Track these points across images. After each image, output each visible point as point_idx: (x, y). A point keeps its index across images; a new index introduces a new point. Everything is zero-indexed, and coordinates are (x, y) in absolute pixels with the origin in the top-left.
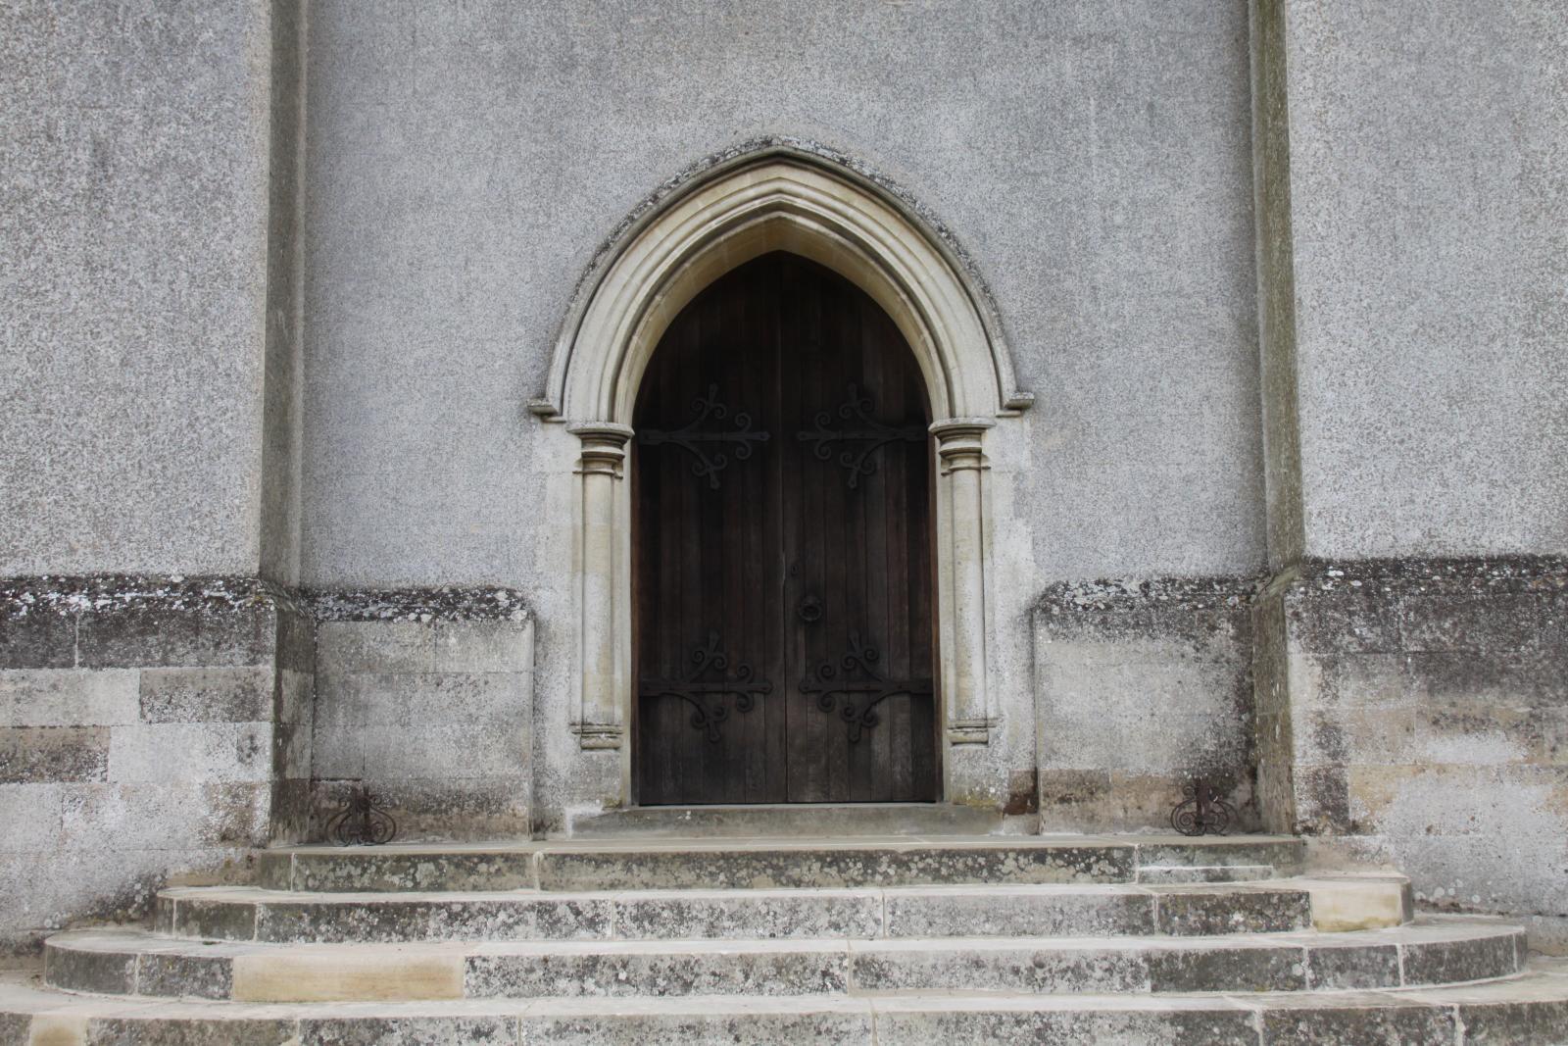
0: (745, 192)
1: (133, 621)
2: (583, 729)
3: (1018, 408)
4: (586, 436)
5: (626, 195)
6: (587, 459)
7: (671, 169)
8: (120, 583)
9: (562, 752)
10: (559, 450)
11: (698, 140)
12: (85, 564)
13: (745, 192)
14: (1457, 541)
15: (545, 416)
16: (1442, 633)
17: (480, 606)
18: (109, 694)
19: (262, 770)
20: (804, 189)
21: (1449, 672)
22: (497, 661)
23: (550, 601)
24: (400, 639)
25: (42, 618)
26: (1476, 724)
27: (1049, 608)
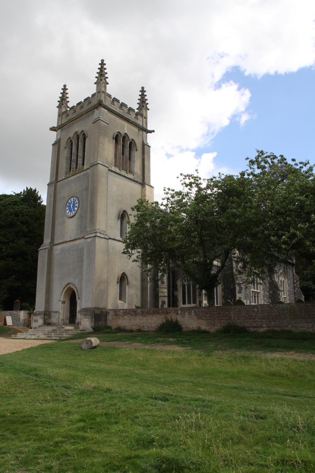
0: (68, 286)
2: (61, 320)
3: (79, 299)
4: (62, 302)
5: (64, 286)
8: (40, 311)
9: (60, 321)
10: (61, 303)
11: (66, 283)
12: (39, 311)
15: (60, 301)
16: (85, 313)
17: (56, 312)
18: (38, 317)
19: (43, 322)
20: (71, 285)
21: (85, 315)
22: (57, 315)
23: (60, 312)
26: (86, 318)
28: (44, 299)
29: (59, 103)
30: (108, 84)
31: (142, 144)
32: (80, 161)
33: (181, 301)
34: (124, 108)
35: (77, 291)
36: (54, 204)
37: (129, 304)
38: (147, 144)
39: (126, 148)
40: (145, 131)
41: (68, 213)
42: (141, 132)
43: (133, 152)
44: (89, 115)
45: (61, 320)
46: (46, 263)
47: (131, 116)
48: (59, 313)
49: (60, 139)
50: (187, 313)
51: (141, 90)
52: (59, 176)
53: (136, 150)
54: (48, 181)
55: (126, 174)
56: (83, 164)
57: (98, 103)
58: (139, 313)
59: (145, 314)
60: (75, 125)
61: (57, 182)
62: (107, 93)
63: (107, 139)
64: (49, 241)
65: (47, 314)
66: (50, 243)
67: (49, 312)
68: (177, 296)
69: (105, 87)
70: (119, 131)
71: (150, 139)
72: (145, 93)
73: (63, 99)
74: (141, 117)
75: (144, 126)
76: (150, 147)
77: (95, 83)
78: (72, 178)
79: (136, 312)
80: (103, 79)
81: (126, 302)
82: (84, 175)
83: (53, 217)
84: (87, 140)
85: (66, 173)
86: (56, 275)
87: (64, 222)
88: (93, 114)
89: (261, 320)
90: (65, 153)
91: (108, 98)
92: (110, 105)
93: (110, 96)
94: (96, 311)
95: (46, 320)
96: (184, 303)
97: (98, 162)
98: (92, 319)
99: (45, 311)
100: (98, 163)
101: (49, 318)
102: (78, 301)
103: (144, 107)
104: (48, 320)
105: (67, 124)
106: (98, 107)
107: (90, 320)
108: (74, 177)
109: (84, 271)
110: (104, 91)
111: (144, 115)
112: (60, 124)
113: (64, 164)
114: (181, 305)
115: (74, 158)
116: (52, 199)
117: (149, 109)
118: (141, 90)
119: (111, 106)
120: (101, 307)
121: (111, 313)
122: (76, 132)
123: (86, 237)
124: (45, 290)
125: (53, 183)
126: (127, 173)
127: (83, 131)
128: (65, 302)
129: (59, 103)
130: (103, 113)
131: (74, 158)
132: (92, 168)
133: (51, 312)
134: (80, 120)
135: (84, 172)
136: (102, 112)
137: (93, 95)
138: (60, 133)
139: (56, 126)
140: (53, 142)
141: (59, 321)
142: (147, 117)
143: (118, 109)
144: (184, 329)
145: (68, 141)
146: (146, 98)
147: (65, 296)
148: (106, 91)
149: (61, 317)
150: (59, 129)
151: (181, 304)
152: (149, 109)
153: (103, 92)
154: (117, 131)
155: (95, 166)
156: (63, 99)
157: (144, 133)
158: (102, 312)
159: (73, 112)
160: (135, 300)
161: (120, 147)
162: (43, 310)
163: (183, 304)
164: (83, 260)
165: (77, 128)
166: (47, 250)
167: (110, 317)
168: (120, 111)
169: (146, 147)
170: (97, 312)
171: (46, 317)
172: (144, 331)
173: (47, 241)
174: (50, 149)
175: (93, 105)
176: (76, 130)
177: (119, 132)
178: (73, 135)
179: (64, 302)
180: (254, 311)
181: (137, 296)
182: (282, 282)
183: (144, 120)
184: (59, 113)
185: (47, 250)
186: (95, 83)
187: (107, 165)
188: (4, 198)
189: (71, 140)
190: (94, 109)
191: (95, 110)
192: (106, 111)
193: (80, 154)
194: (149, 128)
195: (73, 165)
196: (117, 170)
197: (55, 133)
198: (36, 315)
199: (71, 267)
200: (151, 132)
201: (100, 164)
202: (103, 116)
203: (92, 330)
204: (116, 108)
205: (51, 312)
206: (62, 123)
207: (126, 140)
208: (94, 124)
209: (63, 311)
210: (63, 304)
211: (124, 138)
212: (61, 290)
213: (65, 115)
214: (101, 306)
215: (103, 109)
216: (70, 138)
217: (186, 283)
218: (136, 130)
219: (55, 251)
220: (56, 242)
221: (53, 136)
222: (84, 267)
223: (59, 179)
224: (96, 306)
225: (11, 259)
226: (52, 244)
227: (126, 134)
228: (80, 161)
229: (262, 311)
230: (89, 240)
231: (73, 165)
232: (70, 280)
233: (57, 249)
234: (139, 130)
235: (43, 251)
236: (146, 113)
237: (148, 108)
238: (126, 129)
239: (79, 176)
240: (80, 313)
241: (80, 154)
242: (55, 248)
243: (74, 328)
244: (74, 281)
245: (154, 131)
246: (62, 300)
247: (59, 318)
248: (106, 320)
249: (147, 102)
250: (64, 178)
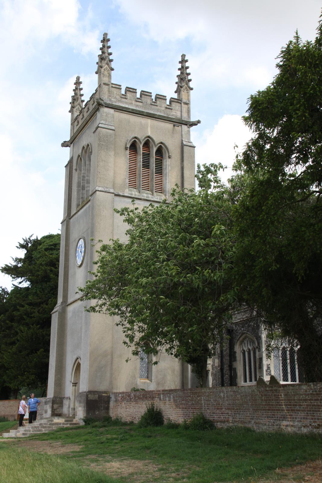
6: (73, 385)
17: (67, 398)
28: (54, 381)
30: (112, 69)
31: (181, 145)
33: (241, 378)
34: (144, 99)
36: (66, 250)
37: (158, 384)
38: (189, 144)
39: (152, 158)
40: (186, 125)
42: (178, 129)
43: (165, 160)
45: (72, 409)
47: (158, 107)
48: (70, 399)
49: (73, 156)
50: (167, 399)
53: (169, 157)
55: (150, 196)
59: (137, 400)
60: (84, 136)
61: (70, 219)
62: (112, 84)
63: (112, 153)
65: (58, 401)
66: (62, 303)
67: (60, 398)
68: (235, 368)
69: (110, 76)
70: (136, 136)
72: (187, 64)
74: (177, 104)
75: (185, 116)
76: (194, 147)
80: (103, 65)
81: (153, 381)
82: (89, 207)
83: (65, 268)
86: (69, 348)
87: (75, 274)
89: (227, 411)
91: (115, 91)
92: (119, 101)
93: (119, 87)
94: (89, 395)
95: (55, 410)
96: (245, 381)
97: (97, 188)
99: (54, 397)
100: (96, 191)
101: (60, 406)
103: (184, 87)
104: (58, 410)
106: (98, 107)
107: (83, 409)
110: (107, 82)
111: (184, 100)
113: (76, 193)
114: (242, 383)
117: (192, 89)
119: (122, 102)
120: (101, 390)
121: (113, 398)
126: (153, 194)
127: (88, 145)
128: (76, 383)
130: (106, 116)
133: (64, 398)
134: (87, 129)
136: (105, 114)
138: (72, 148)
141: (69, 411)
142: (189, 101)
143: (134, 102)
144: (166, 422)
146: (188, 71)
148: (110, 82)
150: (71, 143)
151: (241, 381)
152: (192, 89)
153: (105, 84)
155: (94, 195)
157: (185, 128)
158: (100, 397)
160: (169, 377)
161: (140, 158)
163: (244, 382)
166: (57, 313)
167: (112, 404)
168: (137, 106)
169: (186, 148)
170: (91, 397)
171: (55, 406)
172: (125, 424)
173: (60, 300)
174: (63, 172)
177: (136, 138)
178: (80, 151)
180: (220, 397)
181: (173, 371)
182: (246, 354)
183: (185, 107)
185: (57, 313)
187: (112, 191)
188: (44, 240)
190: (96, 111)
192: (112, 111)
194: (193, 119)
196: (135, 193)
197: (68, 148)
201: (99, 191)
202: (106, 120)
203: (84, 423)
204: (130, 101)
205: (64, 398)
207: (151, 145)
209: (73, 397)
210: (74, 387)
211: (147, 144)
213: (76, 123)
214: (102, 387)
215: (106, 110)
217: (245, 349)
218: (170, 126)
220: (70, 300)
223: (72, 214)
224: (92, 389)
225: (37, 325)
226: (66, 304)
227: (149, 137)
229: (227, 396)
234: (174, 126)
236: (189, 96)
237: (191, 86)
239: (86, 210)
242: (70, 309)
243: (66, 421)
245: (199, 122)
247: (69, 407)
248: (107, 408)
249: (189, 77)
250: (75, 212)
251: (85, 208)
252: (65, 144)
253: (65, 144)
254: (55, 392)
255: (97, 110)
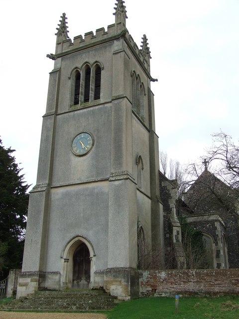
1: (30, 274)
2: (63, 283)
5: (68, 240)
7: (71, 238)
9: (62, 284)
10: (63, 260)
11: (73, 235)
12: (28, 271)
13: (77, 239)
14: (118, 266)
18: (28, 280)
22: (57, 277)
23: (62, 273)
24: (50, 276)
25: (25, 275)
27: (96, 273)
29: (57, 31)
32: (92, 94)
35: (92, 247)
41: (76, 150)
44: (105, 47)
45: (63, 283)
46: (43, 210)
51: (143, 37)
52: (59, 109)
54: (44, 112)
56: (97, 97)
57: (117, 35)
58: (193, 275)
64: (47, 182)
71: (153, 86)
73: (62, 29)
77: (114, 14)
78: (81, 111)
79: (187, 274)
84: (102, 72)
85: (71, 106)
88: (110, 45)
90: (68, 86)
98: (128, 282)
102: (94, 260)
105: (70, 53)
108: (85, 110)
109: (110, 220)
112: (59, 53)
113: (68, 96)
115: (82, 90)
116: (51, 133)
117: (151, 58)
118: (143, 37)
122: (86, 62)
123: (112, 179)
124: (40, 244)
125: (53, 114)
127: (96, 62)
129: (57, 31)
131: (82, 90)
132: (116, 102)
135: (101, 106)
137: (109, 27)
139: (54, 53)
140: (51, 71)
145: (73, 71)
147: (69, 253)
149: (63, 279)
152: (151, 58)
154: (133, 70)
156: (62, 29)
159: (80, 41)
162: (38, 270)
164: (107, 207)
165: (90, 58)
175: (110, 36)
176: (86, 60)
179: (67, 260)
184: (58, 41)
185: (44, 192)
186: (114, 14)
189: (77, 70)
191: (115, 41)
193: (92, 86)
195: (81, 97)
198: (24, 275)
199: (82, 215)
200: (154, 80)
206: (63, 52)
208: (116, 55)
212: (64, 244)
216: (76, 68)
219: (52, 196)
220: (54, 184)
221: (51, 65)
222: (110, 215)
228: (92, 94)
230: (117, 183)
231: (81, 97)
232: (81, 231)
233: (57, 194)
235: (37, 193)
238: (139, 71)
240: (106, 274)
241: (92, 86)
242: (53, 191)
244: (90, 236)
245: (157, 80)
246: (65, 257)
247: (60, 281)
251: (91, 109)
252: (51, 57)
253: (51, 57)
254: (40, 267)
255: (116, 38)
